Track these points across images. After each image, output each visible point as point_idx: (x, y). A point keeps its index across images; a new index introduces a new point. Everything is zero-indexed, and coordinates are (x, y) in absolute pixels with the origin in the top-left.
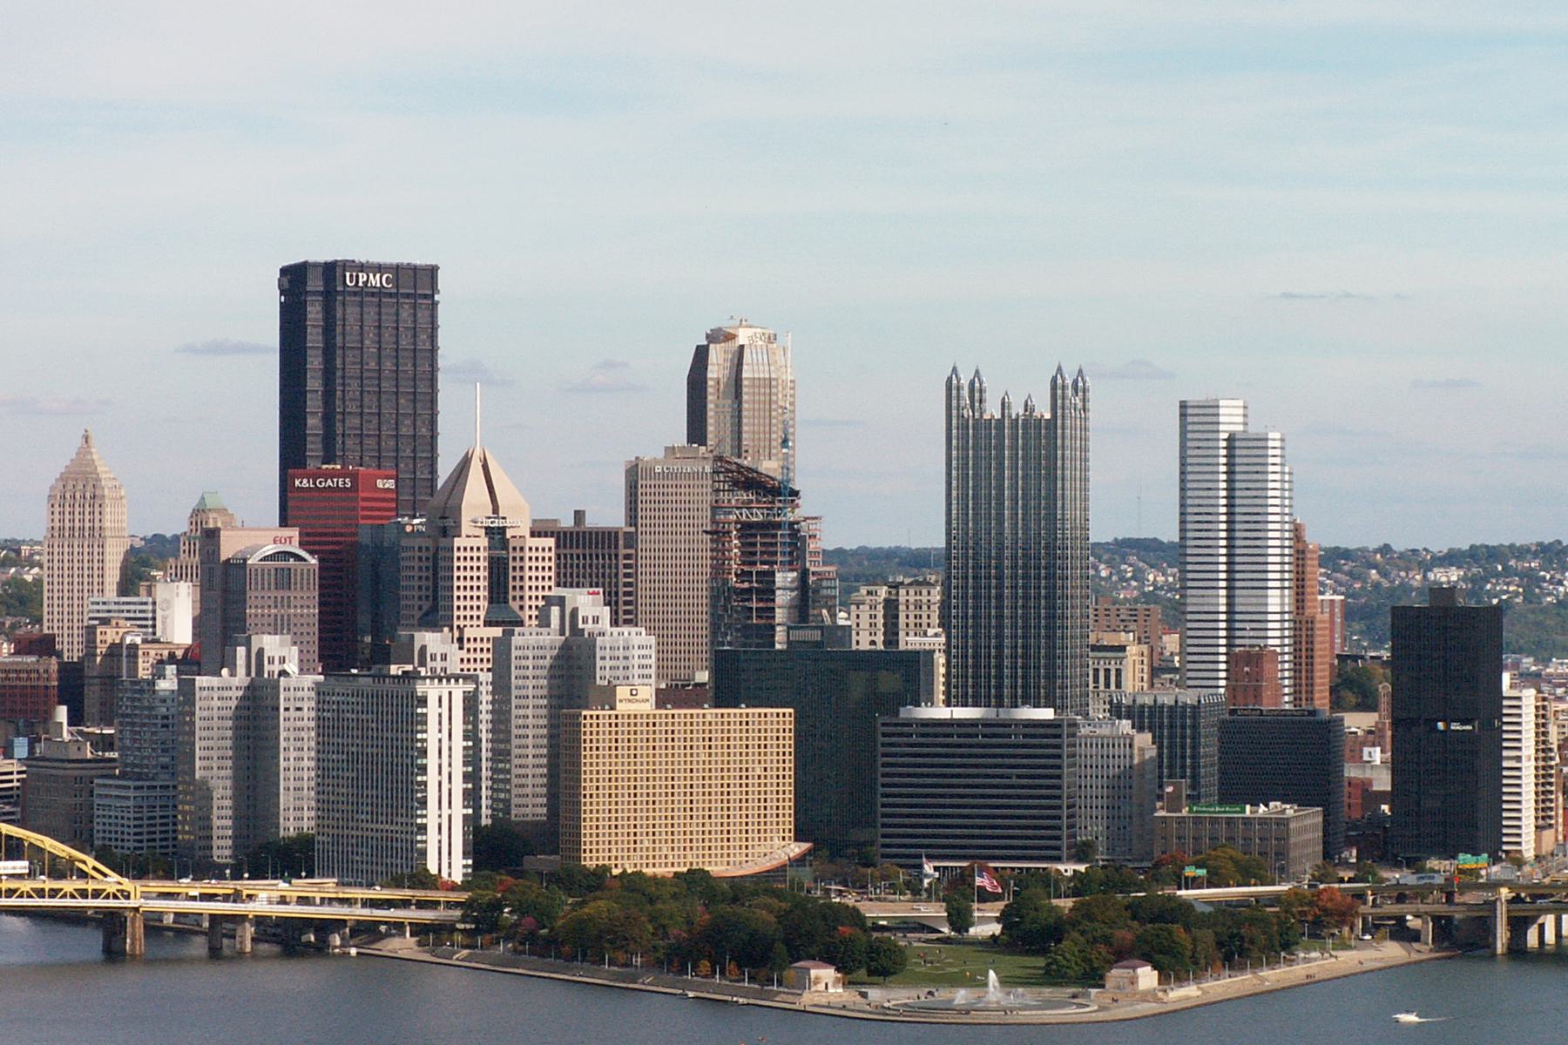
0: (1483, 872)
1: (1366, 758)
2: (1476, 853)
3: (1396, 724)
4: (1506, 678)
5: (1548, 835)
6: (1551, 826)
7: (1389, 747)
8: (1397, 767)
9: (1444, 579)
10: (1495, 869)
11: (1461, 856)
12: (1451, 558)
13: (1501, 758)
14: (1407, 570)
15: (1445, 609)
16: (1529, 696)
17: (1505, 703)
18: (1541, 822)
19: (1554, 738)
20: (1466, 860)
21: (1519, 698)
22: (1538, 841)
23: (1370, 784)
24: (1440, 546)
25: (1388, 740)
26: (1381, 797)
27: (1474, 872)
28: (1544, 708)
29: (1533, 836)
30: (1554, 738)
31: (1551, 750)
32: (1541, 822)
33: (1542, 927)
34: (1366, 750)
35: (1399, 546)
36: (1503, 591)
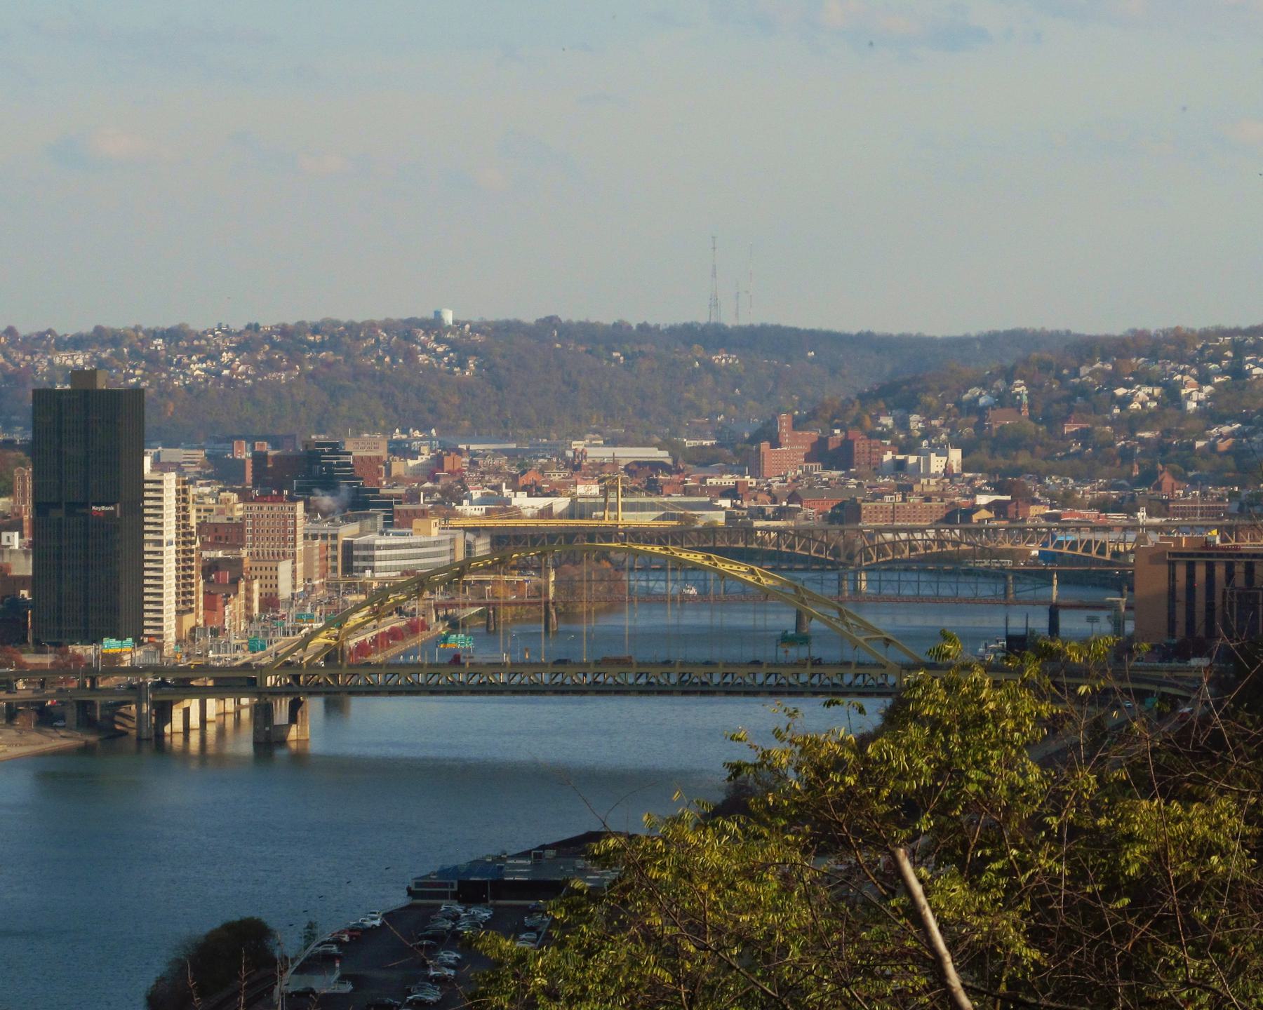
0: (127, 657)
1: (4, 542)
2: (120, 637)
3: (40, 508)
4: (147, 461)
5: (189, 621)
6: (191, 610)
7: (26, 532)
8: (37, 548)
9: (70, 362)
10: (138, 653)
11: (106, 641)
12: (77, 343)
13: (143, 542)
14: (33, 353)
15: (87, 392)
16: (170, 481)
17: (147, 486)
18: (181, 607)
19: (193, 522)
20: (111, 645)
21: (160, 482)
22: (179, 625)
23: (9, 570)
24: (67, 328)
25: (26, 524)
26: (22, 581)
27: (116, 657)
28: (185, 491)
29: (174, 622)
30: (193, 522)
31: (191, 534)
32: (181, 607)
33: (187, 712)
34: (5, 535)
35: (24, 330)
36: (135, 377)
